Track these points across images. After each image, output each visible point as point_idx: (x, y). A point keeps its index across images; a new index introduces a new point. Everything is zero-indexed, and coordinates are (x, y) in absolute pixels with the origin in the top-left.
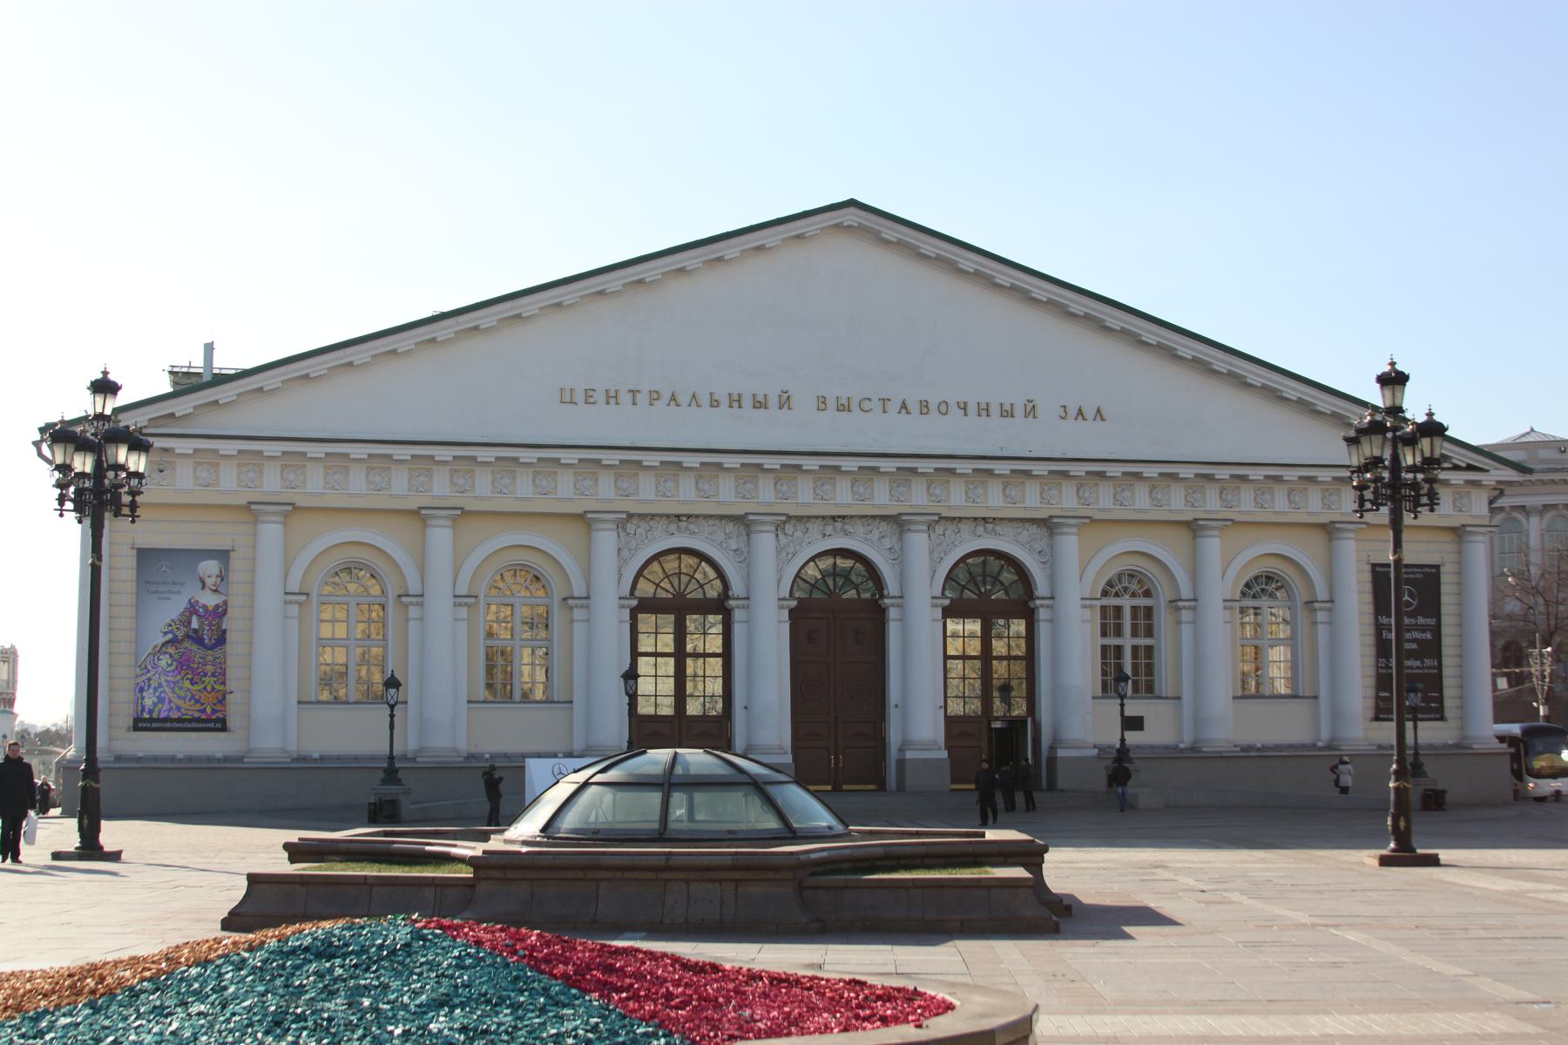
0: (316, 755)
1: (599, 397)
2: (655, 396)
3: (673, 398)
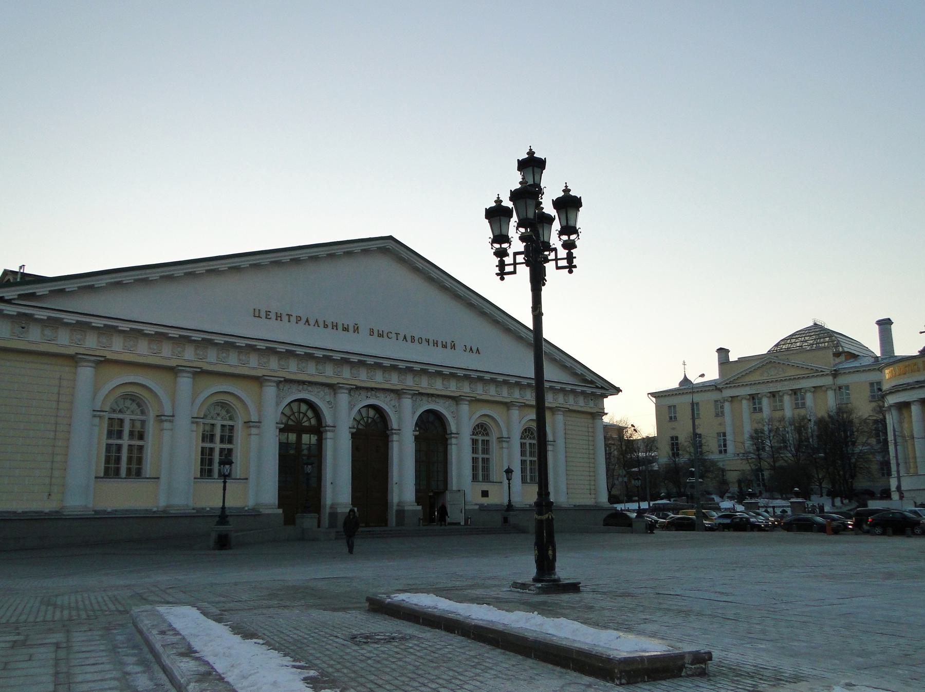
0: (109, 510)
1: (273, 315)
2: (299, 319)
3: (307, 321)
